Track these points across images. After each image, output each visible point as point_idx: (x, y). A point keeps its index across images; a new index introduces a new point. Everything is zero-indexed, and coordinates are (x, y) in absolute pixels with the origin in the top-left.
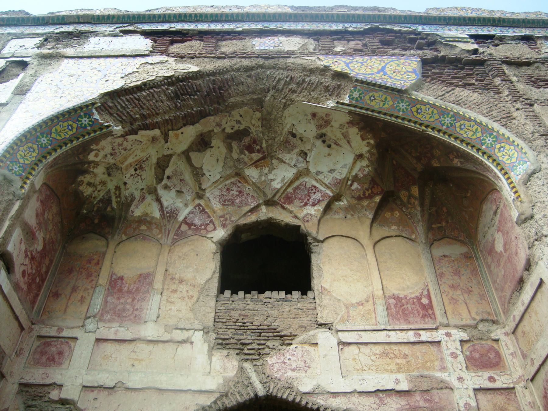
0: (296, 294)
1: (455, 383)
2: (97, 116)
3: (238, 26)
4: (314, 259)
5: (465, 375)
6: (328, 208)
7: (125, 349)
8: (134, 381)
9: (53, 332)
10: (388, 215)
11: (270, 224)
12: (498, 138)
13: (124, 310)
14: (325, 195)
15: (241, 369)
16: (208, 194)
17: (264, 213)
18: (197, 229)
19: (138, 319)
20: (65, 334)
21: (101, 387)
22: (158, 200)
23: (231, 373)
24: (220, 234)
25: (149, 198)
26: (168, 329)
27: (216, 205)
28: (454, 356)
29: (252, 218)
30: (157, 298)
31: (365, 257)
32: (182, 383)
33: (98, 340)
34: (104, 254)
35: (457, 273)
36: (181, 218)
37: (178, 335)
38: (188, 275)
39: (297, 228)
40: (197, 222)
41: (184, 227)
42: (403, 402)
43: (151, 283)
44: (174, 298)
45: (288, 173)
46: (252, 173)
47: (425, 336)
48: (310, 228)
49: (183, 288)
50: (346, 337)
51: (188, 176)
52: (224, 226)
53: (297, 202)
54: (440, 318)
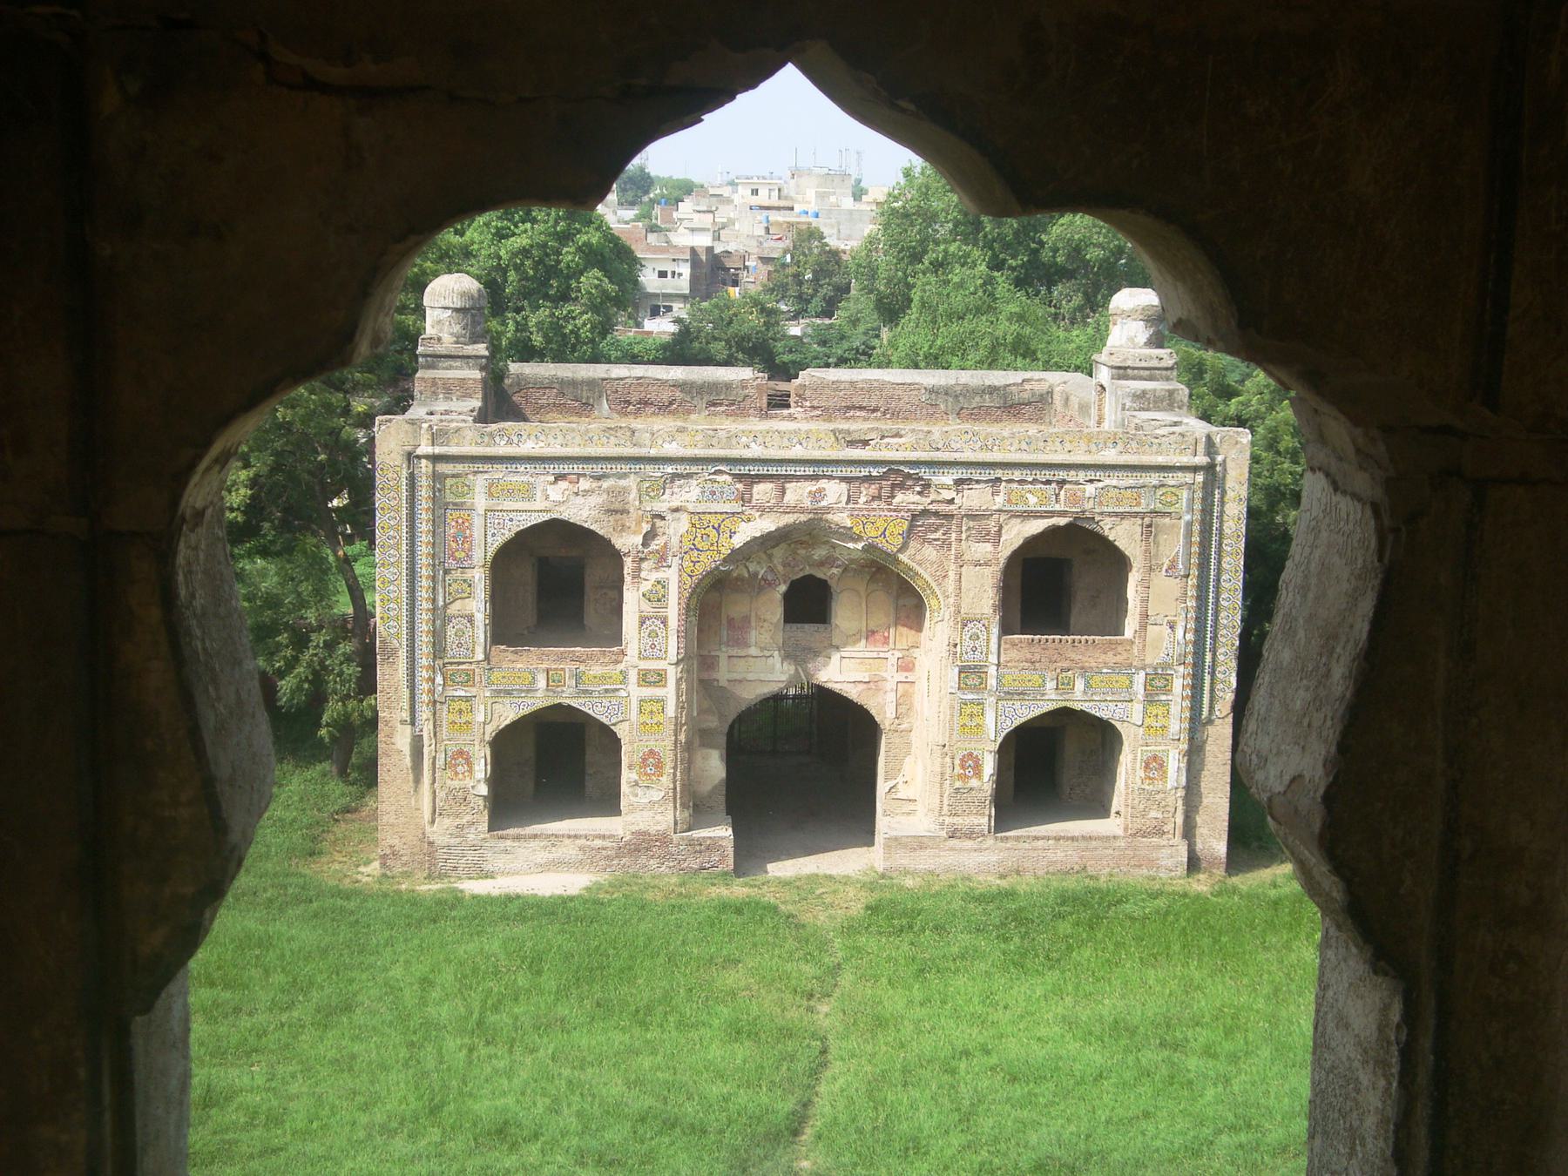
0: (821, 626)
1: (889, 678)
2: (721, 568)
3: (798, 469)
4: (833, 604)
5: (896, 675)
6: (845, 570)
7: (742, 660)
8: (750, 677)
9: (706, 653)
10: (878, 576)
11: (810, 578)
12: (933, 593)
13: (738, 639)
14: (843, 563)
15: (796, 669)
16: (775, 562)
17: (808, 571)
18: (770, 584)
19: (747, 646)
20: (713, 653)
21: (736, 680)
22: (747, 567)
23: (792, 672)
24: (783, 588)
25: (741, 567)
26: (762, 649)
27: (780, 568)
28: (893, 665)
29: (801, 574)
30: (753, 633)
31: (860, 604)
32: (771, 677)
33: (729, 657)
34: (721, 603)
35: (908, 617)
36: (760, 577)
37: (767, 653)
38: (768, 616)
39: (826, 581)
40: (769, 578)
41: (763, 582)
42: (865, 686)
43: (749, 622)
44: (762, 631)
45: (824, 553)
46: (802, 552)
47: (882, 655)
48: (832, 583)
49: (766, 624)
50: (844, 654)
51: (764, 556)
52: (785, 582)
53: (827, 565)
54: (892, 646)
